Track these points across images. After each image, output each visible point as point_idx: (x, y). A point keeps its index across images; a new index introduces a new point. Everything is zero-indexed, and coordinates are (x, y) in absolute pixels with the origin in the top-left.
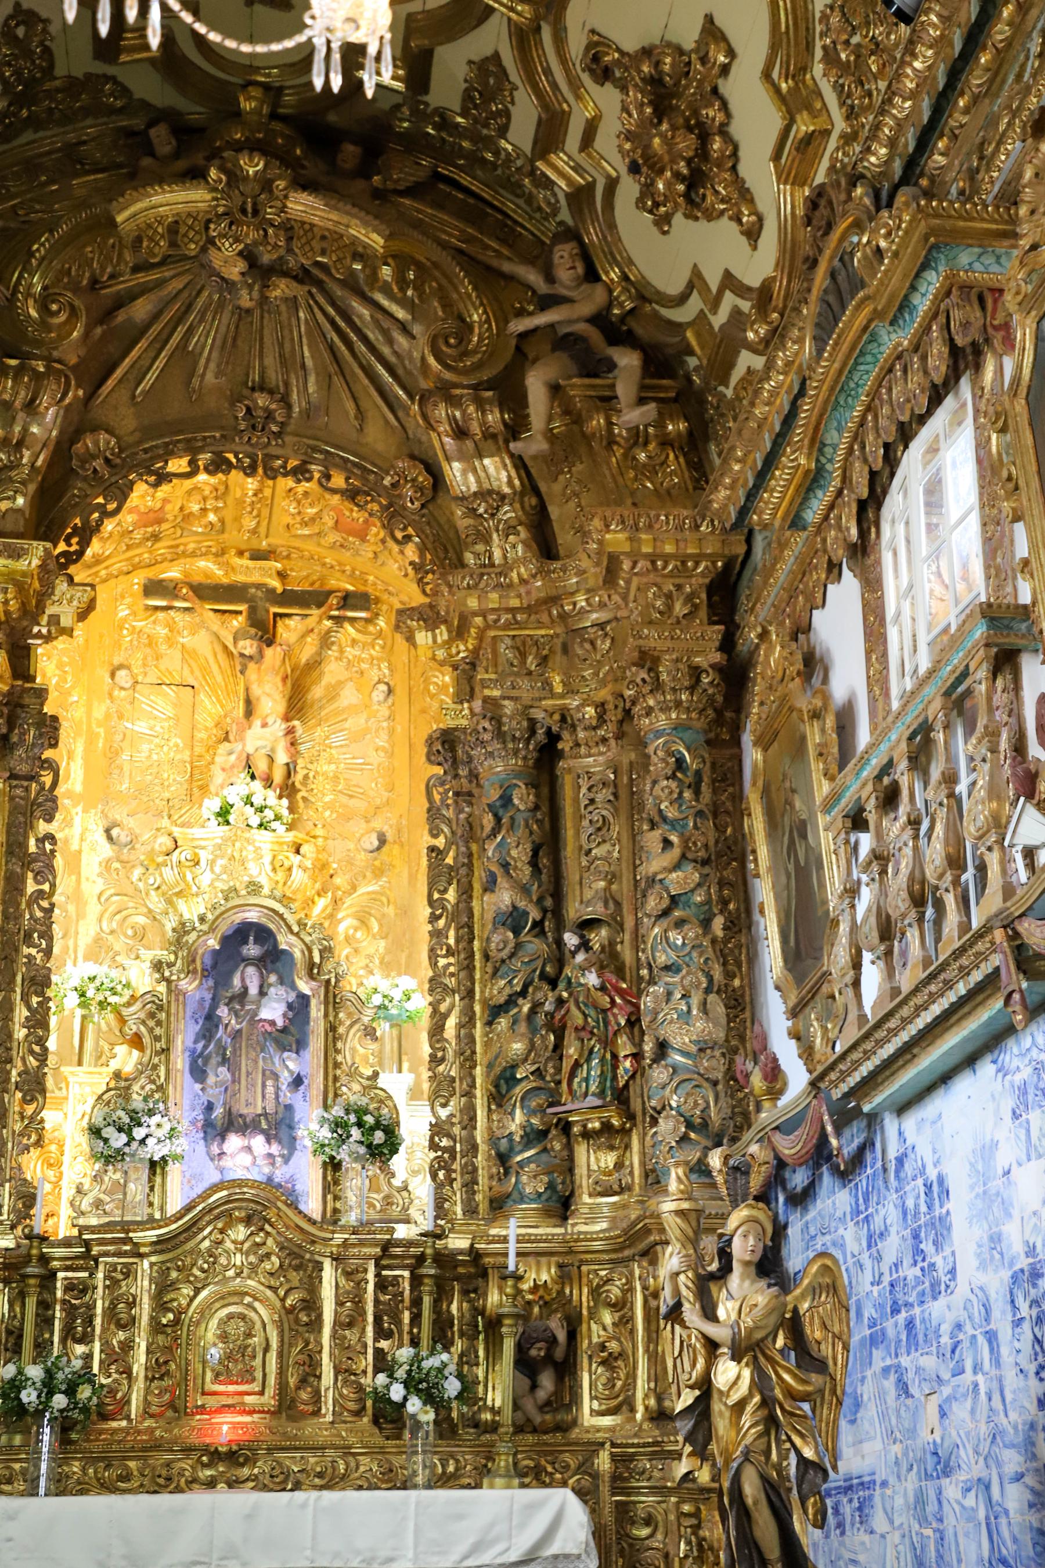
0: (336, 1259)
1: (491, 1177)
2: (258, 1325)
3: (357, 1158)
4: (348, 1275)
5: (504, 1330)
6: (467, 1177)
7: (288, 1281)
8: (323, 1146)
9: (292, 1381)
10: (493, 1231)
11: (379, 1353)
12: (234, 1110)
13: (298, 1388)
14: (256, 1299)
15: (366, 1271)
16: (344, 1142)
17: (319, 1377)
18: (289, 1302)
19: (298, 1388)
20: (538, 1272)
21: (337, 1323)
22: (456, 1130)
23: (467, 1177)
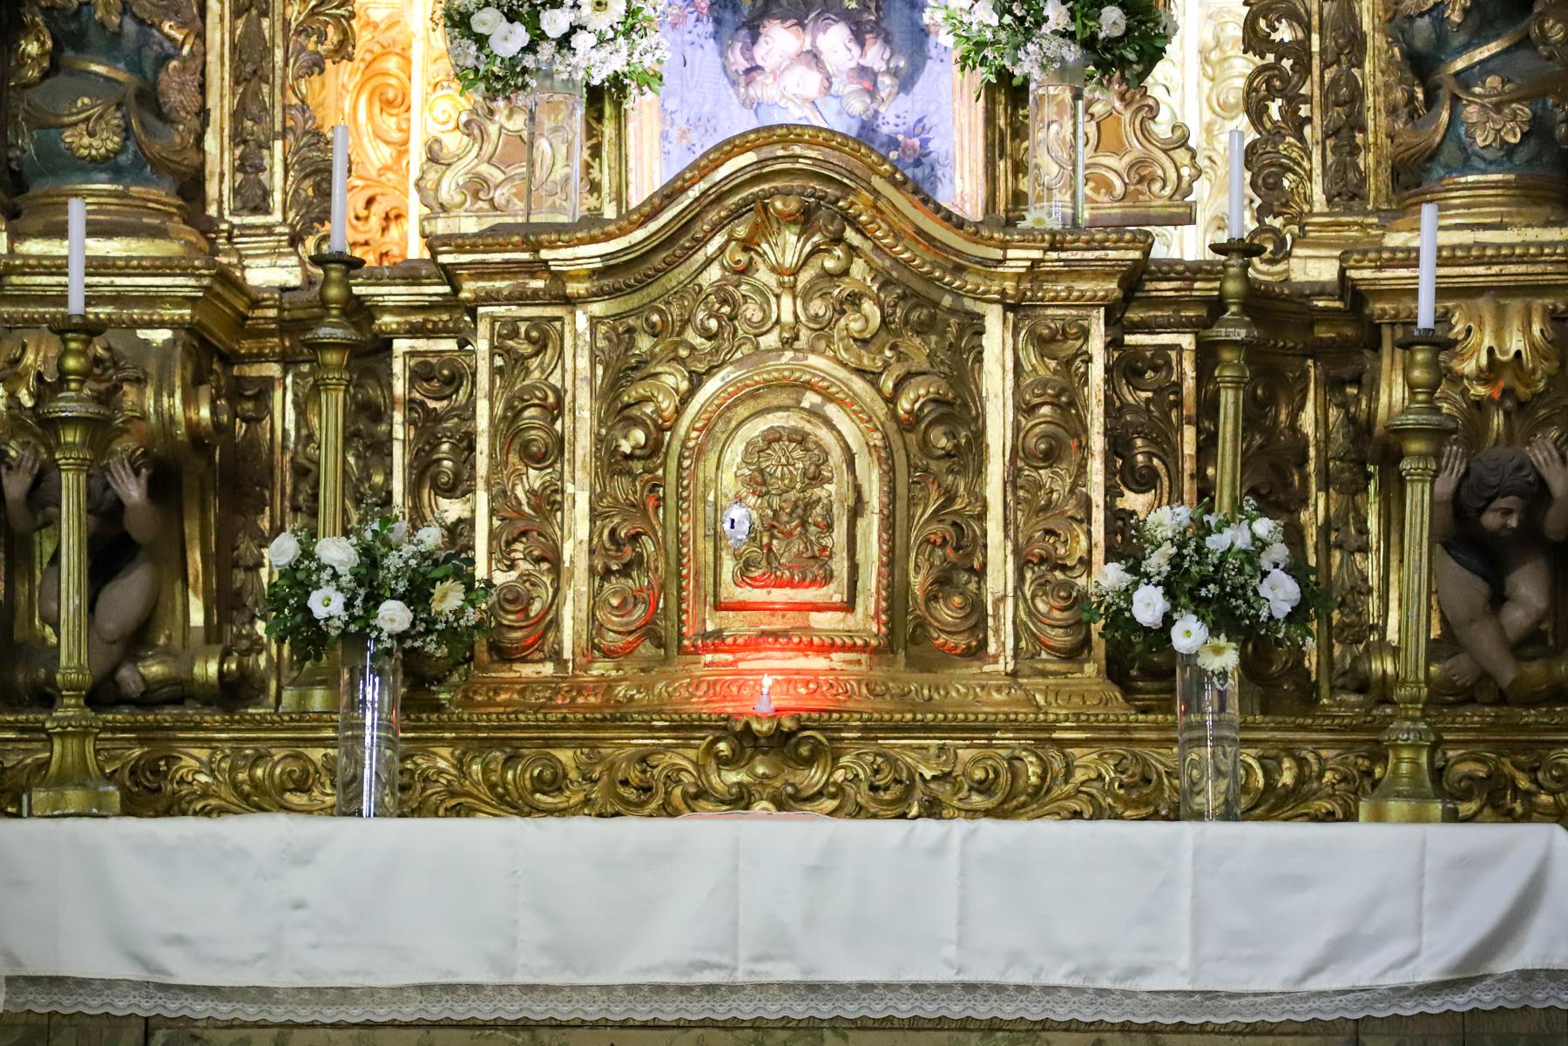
0: (1015, 307)
2: (836, 456)
3: (1064, 72)
4: (1044, 343)
5: (1406, 465)
6: (1338, 113)
7: (901, 357)
8: (980, 45)
13: (931, 598)
14: (829, 398)
15: (1085, 334)
16: (1028, 35)
17: (981, 573)
18: (904, 404)
19: (931, 598)
20: (1499, 333)
21: (1018, 453)
23: (1338, 113)
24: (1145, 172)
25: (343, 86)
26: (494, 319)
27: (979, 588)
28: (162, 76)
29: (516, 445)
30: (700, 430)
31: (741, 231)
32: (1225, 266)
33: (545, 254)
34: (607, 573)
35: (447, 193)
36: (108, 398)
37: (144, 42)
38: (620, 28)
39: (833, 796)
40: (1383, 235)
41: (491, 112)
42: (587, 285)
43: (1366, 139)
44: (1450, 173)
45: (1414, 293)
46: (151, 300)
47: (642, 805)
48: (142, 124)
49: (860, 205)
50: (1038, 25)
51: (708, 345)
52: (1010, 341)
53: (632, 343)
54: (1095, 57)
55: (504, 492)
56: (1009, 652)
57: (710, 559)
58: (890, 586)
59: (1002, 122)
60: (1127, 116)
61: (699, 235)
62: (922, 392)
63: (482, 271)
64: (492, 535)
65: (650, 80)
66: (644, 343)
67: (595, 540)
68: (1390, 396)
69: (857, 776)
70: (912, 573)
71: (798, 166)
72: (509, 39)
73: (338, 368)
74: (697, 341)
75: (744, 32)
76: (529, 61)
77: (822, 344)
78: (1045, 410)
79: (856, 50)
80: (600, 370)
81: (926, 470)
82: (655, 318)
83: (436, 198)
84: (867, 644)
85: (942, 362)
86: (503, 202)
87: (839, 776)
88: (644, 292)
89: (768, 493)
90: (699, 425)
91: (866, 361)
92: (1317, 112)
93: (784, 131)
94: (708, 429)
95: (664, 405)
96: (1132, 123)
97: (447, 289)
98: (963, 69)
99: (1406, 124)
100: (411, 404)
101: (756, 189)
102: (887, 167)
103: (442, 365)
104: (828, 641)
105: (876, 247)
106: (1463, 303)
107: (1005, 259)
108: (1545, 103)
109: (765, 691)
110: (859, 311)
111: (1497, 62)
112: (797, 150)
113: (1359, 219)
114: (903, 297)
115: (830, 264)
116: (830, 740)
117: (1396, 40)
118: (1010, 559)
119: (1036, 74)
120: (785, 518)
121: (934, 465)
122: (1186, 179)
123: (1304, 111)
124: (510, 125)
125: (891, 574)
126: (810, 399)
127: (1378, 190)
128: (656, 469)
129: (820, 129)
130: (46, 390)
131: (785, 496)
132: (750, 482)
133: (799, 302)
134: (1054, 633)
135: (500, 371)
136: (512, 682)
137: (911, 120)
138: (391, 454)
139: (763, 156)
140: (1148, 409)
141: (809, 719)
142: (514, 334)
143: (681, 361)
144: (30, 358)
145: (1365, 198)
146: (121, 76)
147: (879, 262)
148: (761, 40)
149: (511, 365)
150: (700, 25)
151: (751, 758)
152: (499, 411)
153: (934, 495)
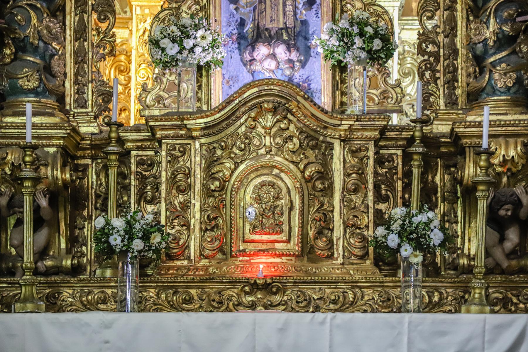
0: (344, 140)
1: (469, 75)
2: (284, 190)
3: (359, 63)
4: (353, 153)
5: (478, 194)
7: (306, 157)
8: (332, 52)
9: (311, 233)
10: (470, 118)
11: (379, 214)
12: (261, 26)
13: (316, 238)
14: (282, 171)
15: (367, 149)
16: (349, 49)
17: (332, 230)
18: (307, 173)
19: (316, 238)
20: (507, 149)
22: (440, 38)
24: (386, 95)
25: (106, 65)
26: (167, 144)
27: (331, 235)
28: (52, 61)
29: (175, 187)
30: (238, 182)
31: (253, 114)
32: (415, 127)
33: (185, 122)
34: (206, 230)
35: (149, 100)
36: (36, 170)
37: (46, 50)
38: (210, 45)
39: (284, 305)
40: (466, 117)
41: (164, 74)
42: (200, 133)
43: (458, 84)
44: (488, 96)
45: (480, 137)
46: (49, 138)
47: (219, 308)
48: (46, 78)
49: (293, 106)
50: (352, 45)
51: (241, 153)
52: (342, 152)
53: (215, 153)
54: (370, 56)
55: (171, 202)
56: (341, 257)
57: (242, 225)
58: (302, 235)
59: (337, 78)
60: (380, 76)
61: (238, 116)
62: (313, 169)
63: (164, 128)
64: (167, 217)
65: (219, 63)
66: (219, 152)
67: (202, 219)
68: (469, 171)
69: (291, 298)
70: (309, 230)
71: (272, 92)
72: (172, 49)
73: (115, 161)
74: (237, 152)
75: (249, 47)
76: (179, 57)
77: (280, 153)
78: (354, 175)
79: (288, 54)
80: (204, 162)
81: (314, 195)
82: (223, 144)
83: (145, 103)
84: (294, 254)
85: (320, 159)
86: (168, 104)
87: (285, 298)
88: (219, 135)
89: (261, 203)
90: (238, 180)
91: (294, 158)
92: (442, 75)
93: (268, 81)
94: (241, 181)
95: (226, 173)
96: (381, 78)
97: (150, 134)
98: (326, 60)
99: (473, 79)
100: (137, 173)
101: (257, 100)
102: (302, 93)
103: (148, 160)
104: (281, 253)
105: (298, 120)
106: (494, 140)
107: (341, 124)
108: (521, 73)
109: (261, 269)
110: (292, 142)
111: (505, 59)
112: (272, 87)
113: (456, 112)
114: (307, 137)
115: (282, 126)
116: (283, 286)
117: (470, 51)
118: (342, 225)
119: (352, 62)
120: (267, 211)
121: (317, 194)
122: (400, 97)
123: (438, 75)
124: (170, 78)
125: (303, 230)
126: (275, 171)
127: (462, 102)
128: (223, 195)
129: (280, 80)
130: (16, 168)
131: (267, 204)
132: (255, 199)
133: (272, 138)
134: (356, 250)
135: (170, 162)
136: (174, 267)
137: (304, 77)
138: (130, 190)
139: (260, 89)
140: (386, 175)
141: (276, 279)
142: (174, 149)
143: (232, 158)
144: (9, 157)
145: (458, 105)
146: (38, 61)
147: (299, 125)
148: (256, 50)
149: (173, 160)
150: (233, 45)
151: (256, 292)
152: (169, 175)
153: (317, 204)
